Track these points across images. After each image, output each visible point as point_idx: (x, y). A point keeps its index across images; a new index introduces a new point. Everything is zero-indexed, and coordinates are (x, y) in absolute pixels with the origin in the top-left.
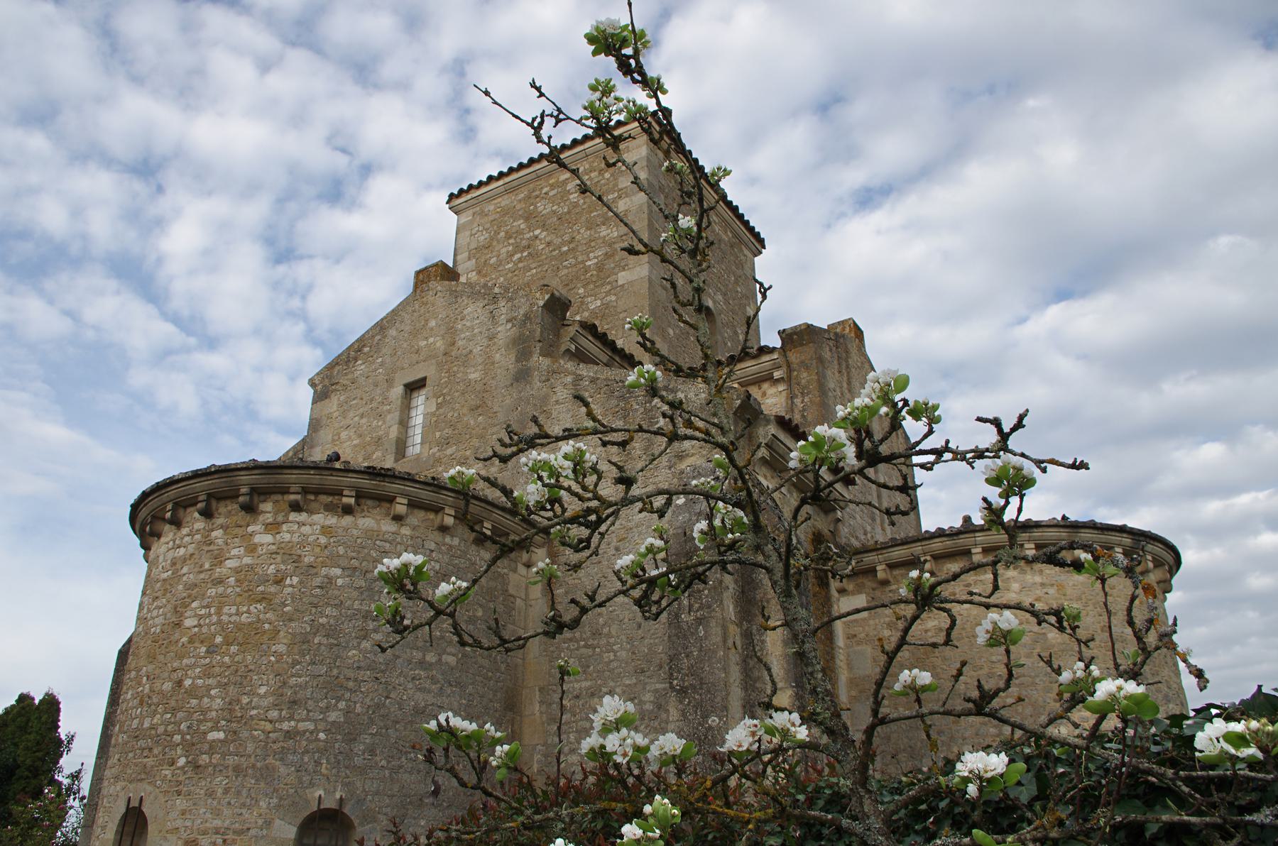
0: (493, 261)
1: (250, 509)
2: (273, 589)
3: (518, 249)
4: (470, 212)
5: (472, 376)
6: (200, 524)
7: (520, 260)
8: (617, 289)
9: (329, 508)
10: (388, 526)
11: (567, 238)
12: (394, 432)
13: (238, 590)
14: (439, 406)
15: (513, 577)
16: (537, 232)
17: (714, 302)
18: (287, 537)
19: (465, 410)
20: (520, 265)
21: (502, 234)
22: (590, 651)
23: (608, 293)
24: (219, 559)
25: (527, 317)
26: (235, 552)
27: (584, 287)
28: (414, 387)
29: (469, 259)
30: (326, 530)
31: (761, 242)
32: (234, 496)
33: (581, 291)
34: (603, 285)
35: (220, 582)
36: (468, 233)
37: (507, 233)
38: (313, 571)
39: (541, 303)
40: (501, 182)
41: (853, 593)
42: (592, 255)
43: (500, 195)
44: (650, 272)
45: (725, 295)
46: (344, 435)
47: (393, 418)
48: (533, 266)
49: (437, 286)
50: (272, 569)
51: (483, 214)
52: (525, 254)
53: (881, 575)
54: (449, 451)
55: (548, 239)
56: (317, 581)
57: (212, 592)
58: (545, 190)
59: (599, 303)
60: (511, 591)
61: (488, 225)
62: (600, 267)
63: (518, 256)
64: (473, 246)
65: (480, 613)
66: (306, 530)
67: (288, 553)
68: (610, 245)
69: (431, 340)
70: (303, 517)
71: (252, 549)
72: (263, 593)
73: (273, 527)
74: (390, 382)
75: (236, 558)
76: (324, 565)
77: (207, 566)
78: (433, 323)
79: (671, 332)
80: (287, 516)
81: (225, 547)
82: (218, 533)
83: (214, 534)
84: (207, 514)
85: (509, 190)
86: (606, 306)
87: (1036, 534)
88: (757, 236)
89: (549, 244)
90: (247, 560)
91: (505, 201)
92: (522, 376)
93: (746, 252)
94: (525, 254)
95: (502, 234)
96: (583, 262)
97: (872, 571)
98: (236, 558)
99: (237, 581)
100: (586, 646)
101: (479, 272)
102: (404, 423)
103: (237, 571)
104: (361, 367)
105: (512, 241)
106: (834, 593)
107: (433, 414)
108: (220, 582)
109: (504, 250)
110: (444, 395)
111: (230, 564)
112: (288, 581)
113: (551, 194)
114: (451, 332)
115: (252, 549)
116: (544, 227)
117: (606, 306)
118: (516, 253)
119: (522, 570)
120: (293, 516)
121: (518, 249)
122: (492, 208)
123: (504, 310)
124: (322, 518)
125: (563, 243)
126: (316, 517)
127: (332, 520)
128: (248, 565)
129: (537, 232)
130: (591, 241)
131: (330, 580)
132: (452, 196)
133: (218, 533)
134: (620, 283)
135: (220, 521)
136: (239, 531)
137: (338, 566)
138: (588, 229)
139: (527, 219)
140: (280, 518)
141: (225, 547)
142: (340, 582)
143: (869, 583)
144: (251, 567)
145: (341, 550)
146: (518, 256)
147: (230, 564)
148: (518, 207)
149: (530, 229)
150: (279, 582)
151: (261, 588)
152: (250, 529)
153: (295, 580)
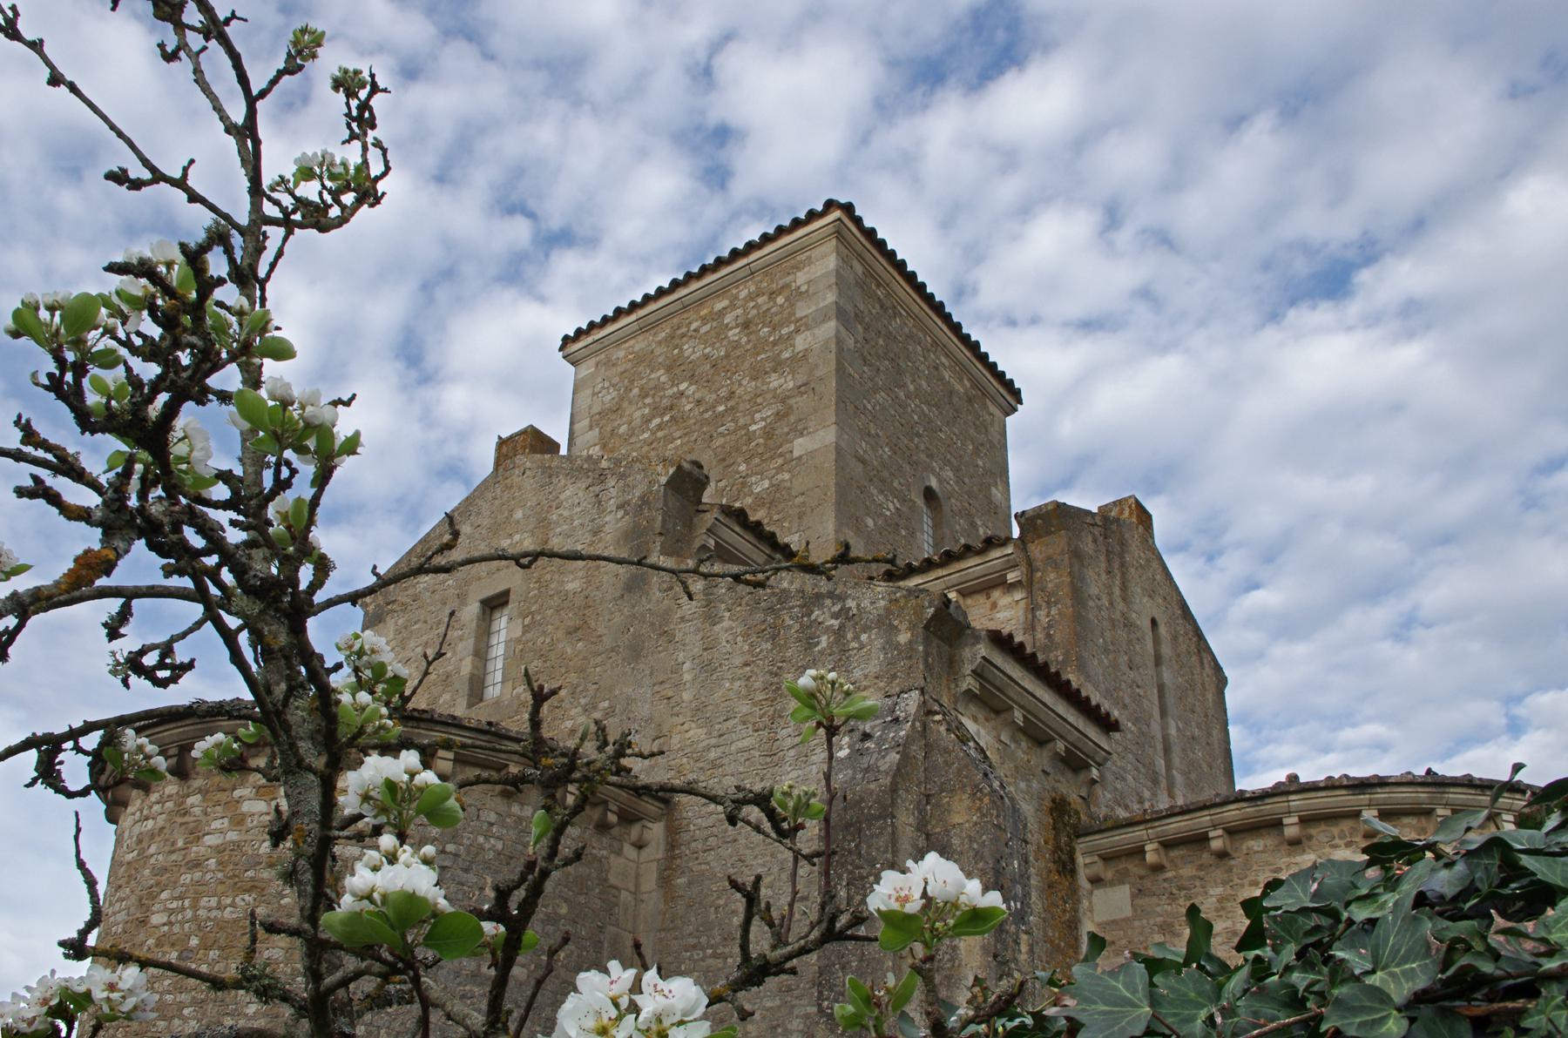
0: (623, 429)
3: (657, 411)
4: (592, 362)
5: (570, 586)
7: (660, 427)
8: (791, 463)
11: (723, 393)
12: (467, 667)
13: (220, 875)
14: (526, 629)
15: (616, 862)
16: (683, 386)
17: (940, 480)
19: (560, 634)
20: (660, 434)
21: (636, 391)
22: (719, 963)
23: (780, 469)
24: (195, 835)
25: (644, 501)
26: (216, 824)
27: (746, 461)
28: (495, 604)
29: (591, 428)
31: (1016, 394)
33: (743, 468)
34: (772, 458)
36: (589, 392)
37: (642, 389)
39: (664, 480)
40: (633, 317)
41: (1112, 884)
42: (757, 416)
43: (633, 336)
44: (839, 437)
45: (957, 470)
49: (525, 461)
51: (610, 364)
52: (667, 418)
53: (1150, 857)
59: (766, 484)
60: (613, 880)
62: (768, 433)
63: (657, 421)
64: (596, 409)
65: (564, 910)
68: (783, 401)
69: (517, 537)
71: (238, 821)
72: (252, 879)
75: (219, 832)
77: (180, 844)
79: (870, 522)
81: (203, 818)
83: (190, 800)
85: (645, 328)
86: (777, 487)
87: (1381, 795)
88: (1009, 385)
89: (699, 402)
90: (232, 836)
91: (639, 344)
93: (993, 409)
94: (667, 418)
95: (636, 391)
96: (746, 426)
97: (1139, 852)
98: (219, 832)
99: (219, 863)
100: (715, 956)
101: (604, 447)
102: (481, 654)
103: (219, 850)
105: (648, 400)
106: (1084, 883)
107: (518, 641)
110: (532, 613)
111: (210, 840)
113: (703, 330)
115: (238, 821)
116: (692, 378)
117: (777, 487)
118: (654, 417)
119: (630, 851)
121: (657, 411)
122: (621, 354)
123: (613, 492)
125: (718, 402)
128: (233, 842)
129: (683, 386)
130: (757, 396)
132: (566, 339)
134: (796, 454)
136: (223, 797)
138: (754, 378)
139: (669, 369)
141: (203, 818)
143: (1134, 868)
144: (237, 845)
146: (657, 421)
147: (210, 840)
148: (658, 351)
149: (674, 382)
151: (250, 874)
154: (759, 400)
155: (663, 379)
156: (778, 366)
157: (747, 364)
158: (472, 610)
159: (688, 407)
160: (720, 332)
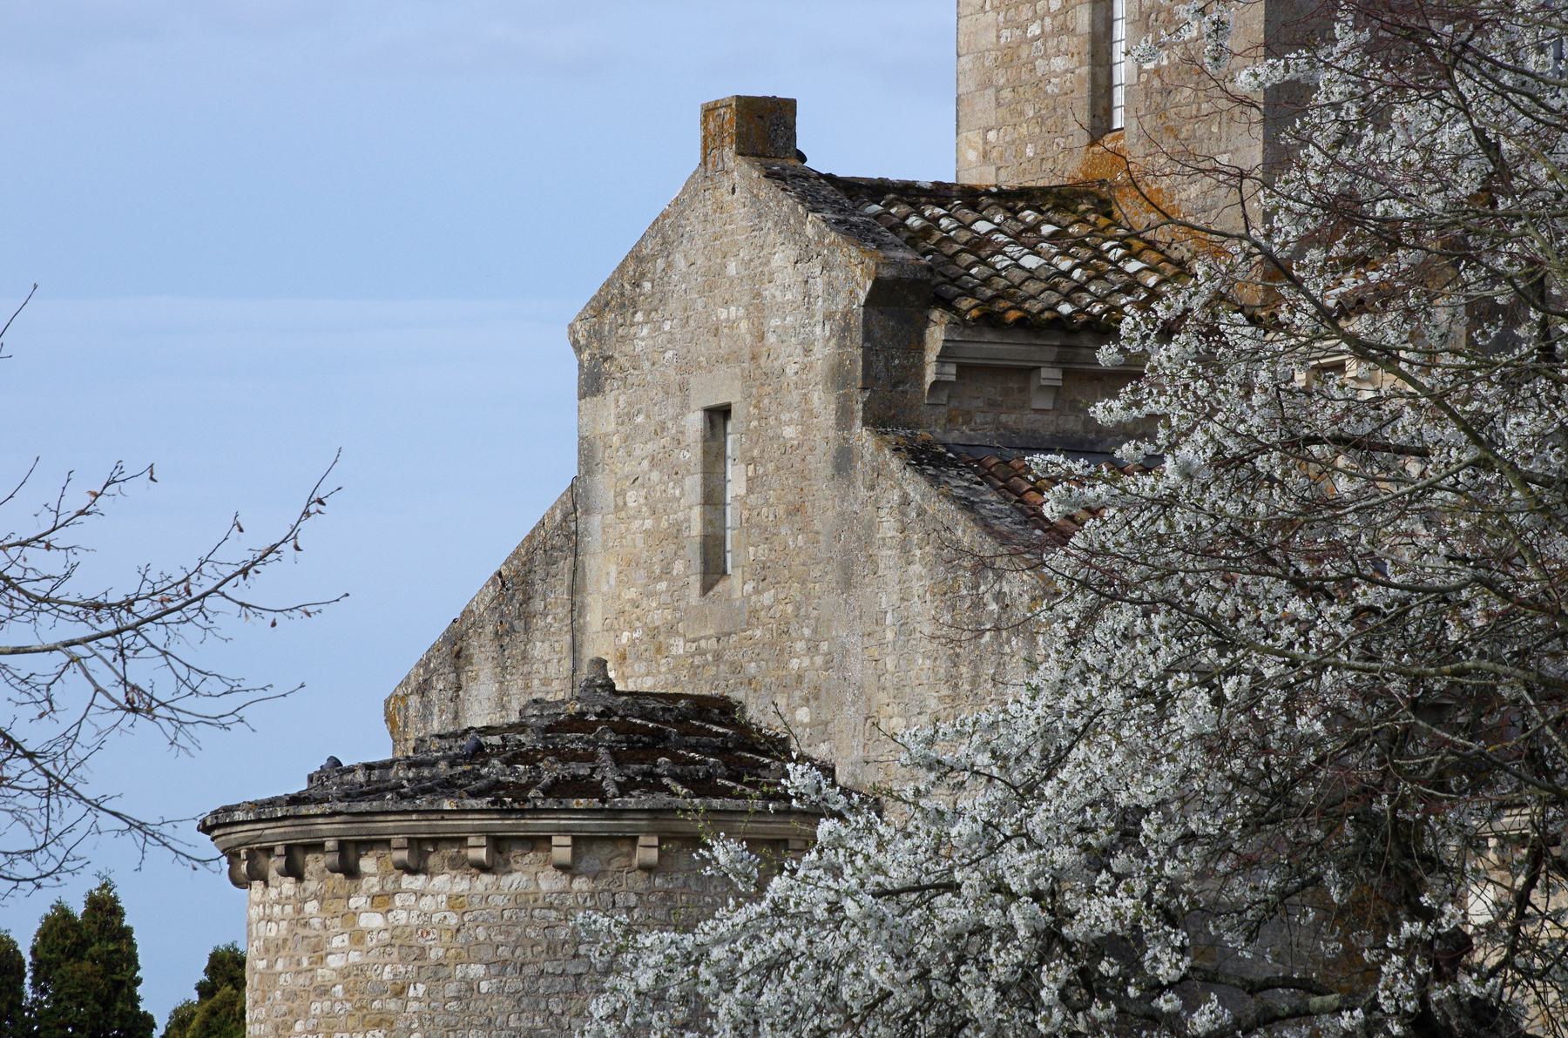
1: (351, 871)
2: (392, 1005)
6: (288, 885)
9: (458, 864)
10: (549, 882)
12: (696, 528)
13: (348, 1006)
18: (402, 916)
24: (319, 954)
30: (456, 903)
32: (318, 847)
35: (324, 991)
38: (443, 973)
46: (631, 496)
47: (693, 484)
50: (387, 974)
54: (767, 598)
56: (451, 989)
57: (316, 1008)
66: (427, 903)
67: (404, 944)
70: (419, 882)
71: (358, 938)
72: (380, 1012)
73: (381, 902)
74: (685, 407)
76: (459, 960)
77: (305, 963)
78: (732, 269)
80: (397, 880)
81: (322, 932)
82: (311, 907)
84: (294, 870)
90: (355, 957)
92: (844, 461)
99: (346, 991)
102: (713, 498)
103: (344, 974)
104: (643, 337)
108: (324, 991)
111: (334, 961)
112: (411, 993)
114: (758, 308)
115: (358, 938)
120: (407, 881)
124: (446, 883)
126: (440, 881)
127: (462, 885)
128: (355, 965)
131: (471, 986)
133: (311, 907)
135: (312, 885)
137: (480, 961)
140: (389, 887)
141: (322, 932)
142: (484, 986)
144: (360, 968)
145: (481, 934)
150: (400, 993)
151: (377, 1004)
152: (353, 903)
153: (421, 988)
158: (695, 422)
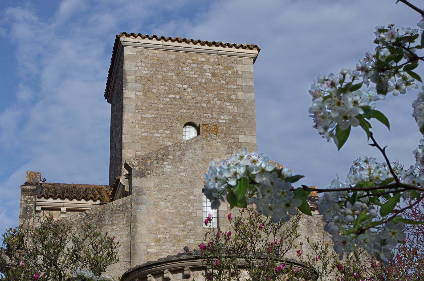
16: (185, 86)
21: (160, 76)
37: (163, 76)
48: (184, 107)
55: (193, 94)
58: (189, 61)
61: (149, 65)
68: (233, 116)
89: (194, 98)
91: (161, 54)
101: (145, 94)
105: (167, 84)
109: (161, 87)
113: (193, 65)
129: (185, 86)
139: (177, 75)
154: (222, 110)
155: (174, 78)
156: (230, 100)
157: (216, 92)
159: (188, 97)
160: (202, 72)
